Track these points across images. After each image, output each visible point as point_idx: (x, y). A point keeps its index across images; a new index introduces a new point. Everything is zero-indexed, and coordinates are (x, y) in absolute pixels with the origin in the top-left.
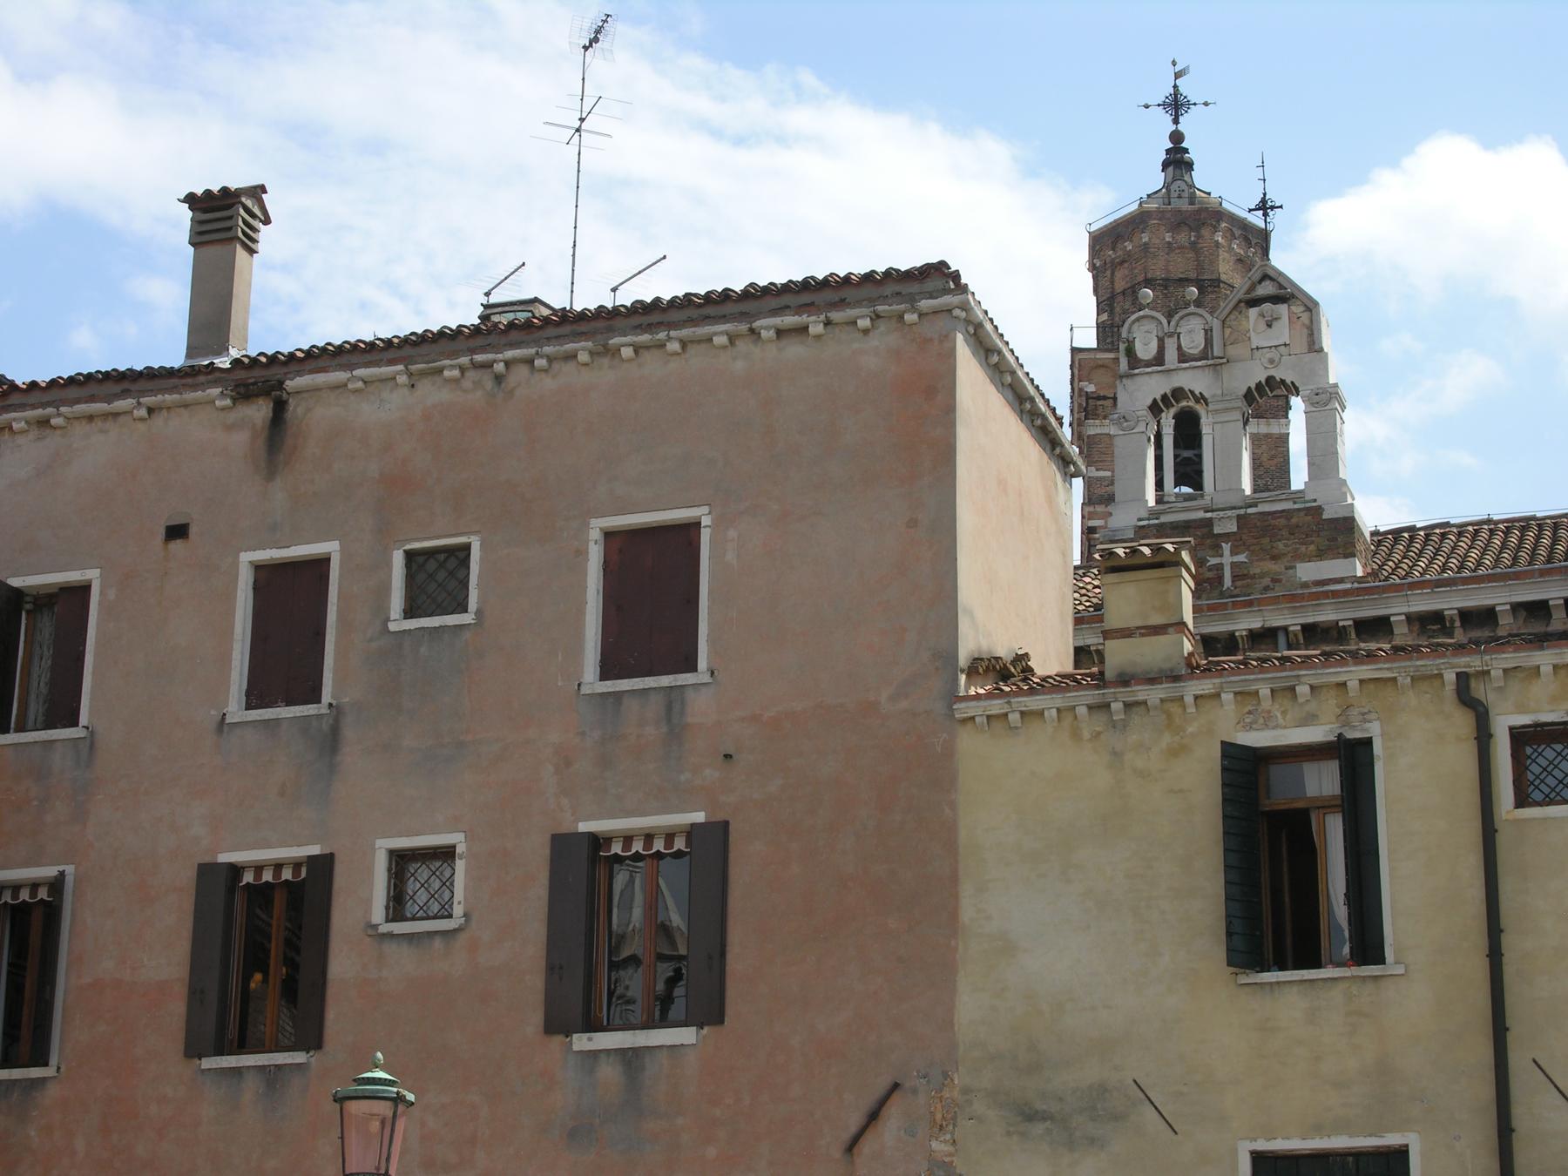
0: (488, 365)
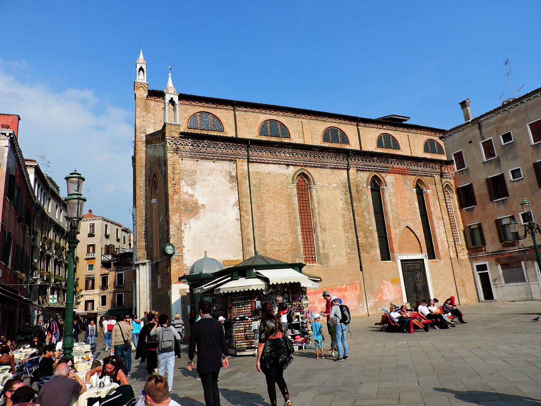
0: (506, 110)
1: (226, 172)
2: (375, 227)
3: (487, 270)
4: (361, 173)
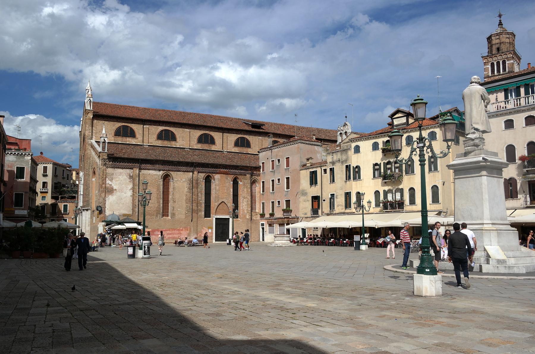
1: (128, 174)
2: (204, 201)
3: (264, 226)
4: (200, 174)
